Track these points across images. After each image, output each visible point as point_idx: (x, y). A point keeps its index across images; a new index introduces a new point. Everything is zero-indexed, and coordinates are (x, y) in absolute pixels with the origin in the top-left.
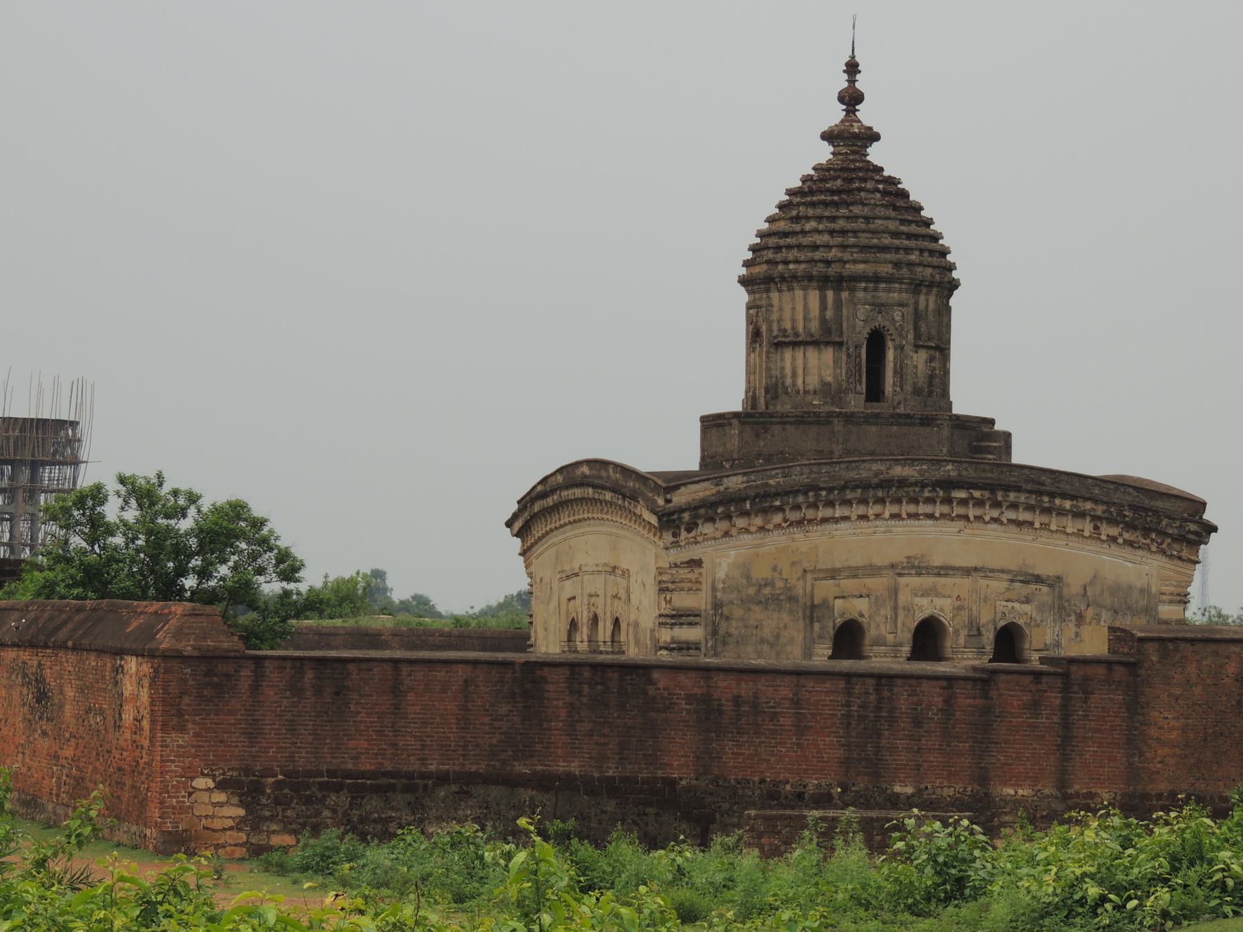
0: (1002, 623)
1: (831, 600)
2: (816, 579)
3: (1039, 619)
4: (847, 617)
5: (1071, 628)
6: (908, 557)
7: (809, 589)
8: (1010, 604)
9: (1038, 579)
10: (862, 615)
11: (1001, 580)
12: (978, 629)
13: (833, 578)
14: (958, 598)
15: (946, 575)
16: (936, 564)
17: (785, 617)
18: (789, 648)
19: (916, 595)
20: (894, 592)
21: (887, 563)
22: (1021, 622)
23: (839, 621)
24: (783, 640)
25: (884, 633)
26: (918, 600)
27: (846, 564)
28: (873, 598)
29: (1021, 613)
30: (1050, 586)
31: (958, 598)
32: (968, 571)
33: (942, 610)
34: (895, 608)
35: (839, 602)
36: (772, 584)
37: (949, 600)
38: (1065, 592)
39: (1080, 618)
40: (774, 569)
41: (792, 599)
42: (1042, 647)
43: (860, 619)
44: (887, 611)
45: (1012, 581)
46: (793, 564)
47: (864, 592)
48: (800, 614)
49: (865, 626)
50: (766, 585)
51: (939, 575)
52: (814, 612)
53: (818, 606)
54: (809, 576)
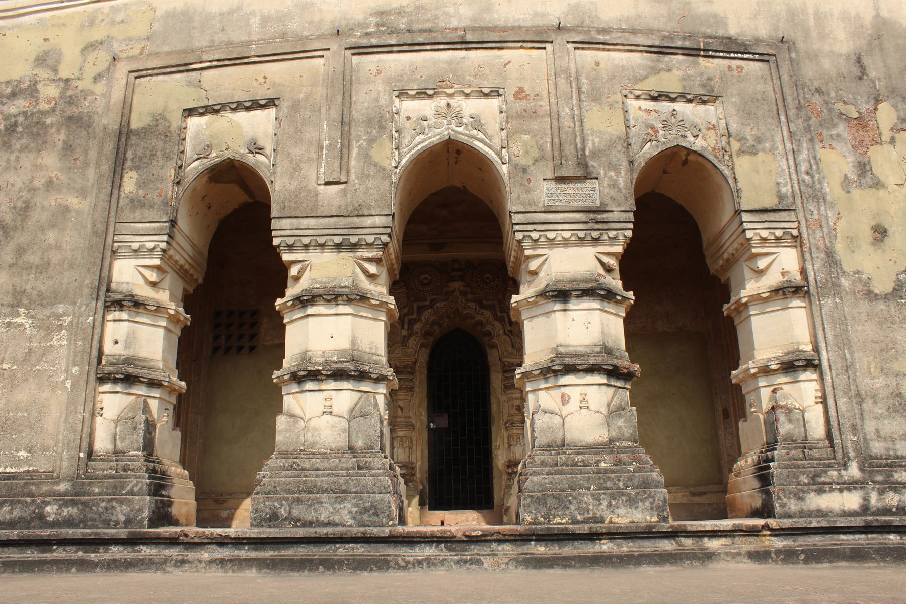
0: (650, 150)
1: (175, 120)
2: (139, 73)
3: (749, 133)
4: (215, 157)
5: (837, 161)
6: (382, 13)
7: (117, 94)
8: (665, 106)
9: (733, 48)
10: (260, 150)
11: (633, 48)
12: (582, 163)
13: (183, 68)
14: (520, 93)
15: (482, 44)
16: (454, 23)
17: (50, 160)
18: (51, 236)
19: (402, 94)
20: (344, 86)
21: (326, 28)
22: (698, 144)
23: (195, 167)
24: (37, 216)
25: (312, 184)
26: (411, 107)
27: (220, 38)
28: (284, 105)
29: (701, 127)
30: (763, 58)
31: (520, 93)
32: (537, 39)
33: (477, 123)
34: (345, 123)
35: (194, 122)
36: (32, 91)
37: (495, 102)
38: (808, 71)
39: (861, 123)
40: (41, 60)
41: (77, 122)
42: (769, 201)
43: (250, 159)
44: (325, 132)
45: (662, 51)
46: (90, 47)
47: (262, 94)
48: (93, 154)
49: (265, 174)
50: (13, 95)
51: (463, 44)
52: (126, 144)
53: (145, 132)
54: (122, 70)
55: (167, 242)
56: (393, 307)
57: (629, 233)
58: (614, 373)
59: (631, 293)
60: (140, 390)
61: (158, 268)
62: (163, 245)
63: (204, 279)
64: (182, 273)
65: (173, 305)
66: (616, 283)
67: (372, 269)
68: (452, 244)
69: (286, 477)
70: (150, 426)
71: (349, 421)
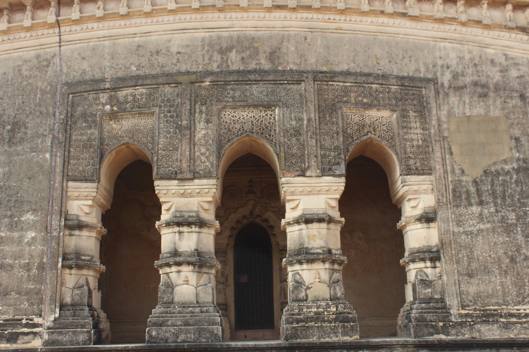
55: (97, 192)
56: (218, 227)
57: (343, 188)
58: (333, 262)
59: (343, 218)
60: (85, 272)
61: (90, 206)
62: (94, 194)
63: (111, 206)
64: (101, 206)
65: (99, 225)
66: (336, 214)
67: (206, 206)
68: (250, 184)
69: (162, 317)
70: (90, 292)
71: (196, 288)
